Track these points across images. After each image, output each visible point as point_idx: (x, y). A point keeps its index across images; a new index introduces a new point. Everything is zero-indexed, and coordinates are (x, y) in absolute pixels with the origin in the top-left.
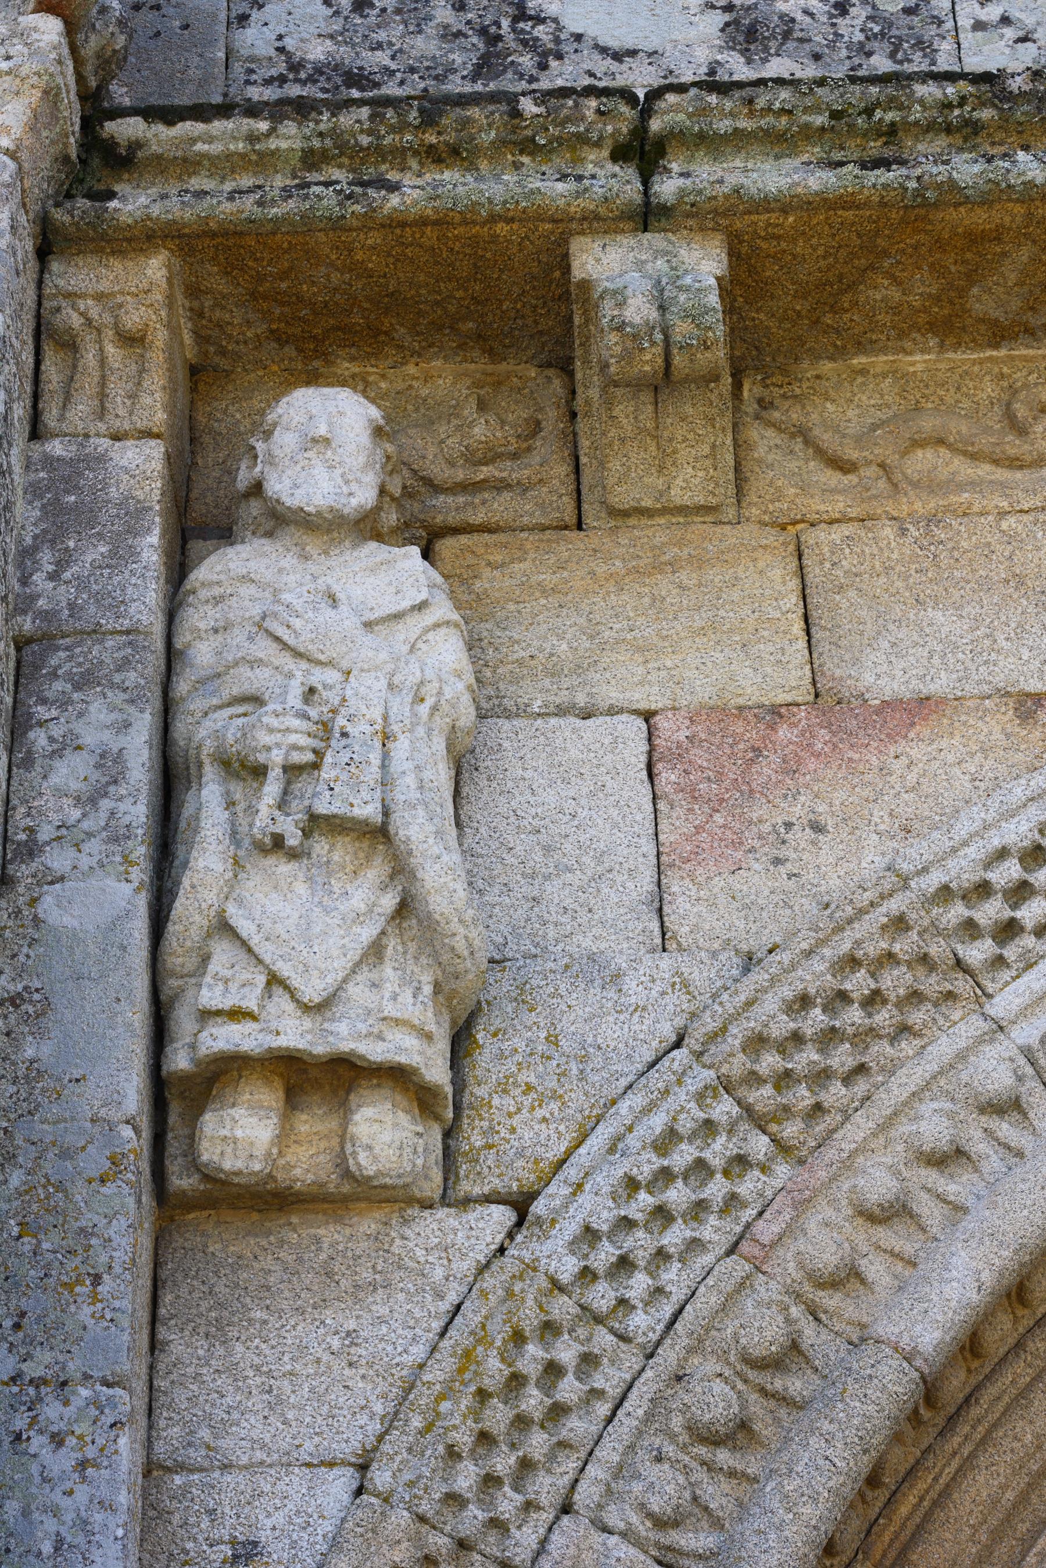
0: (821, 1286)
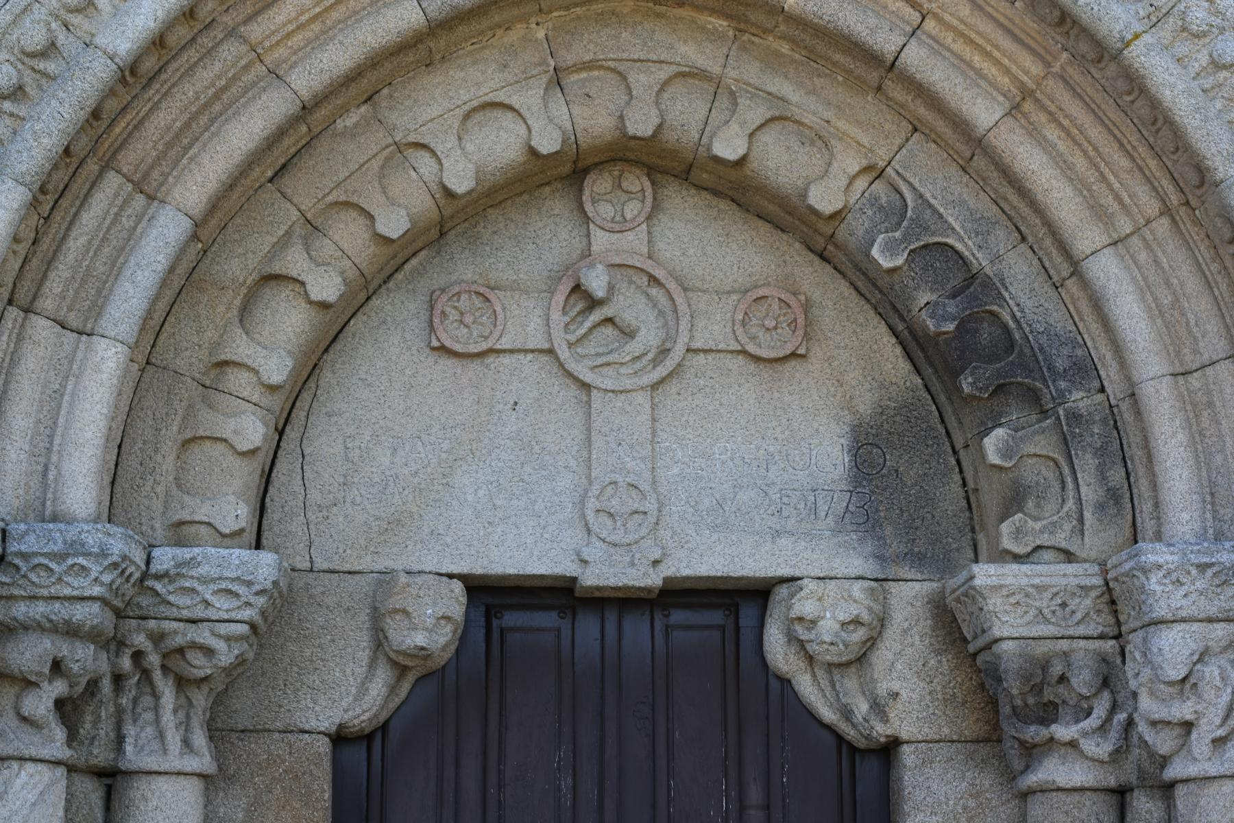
0: (71, 12)
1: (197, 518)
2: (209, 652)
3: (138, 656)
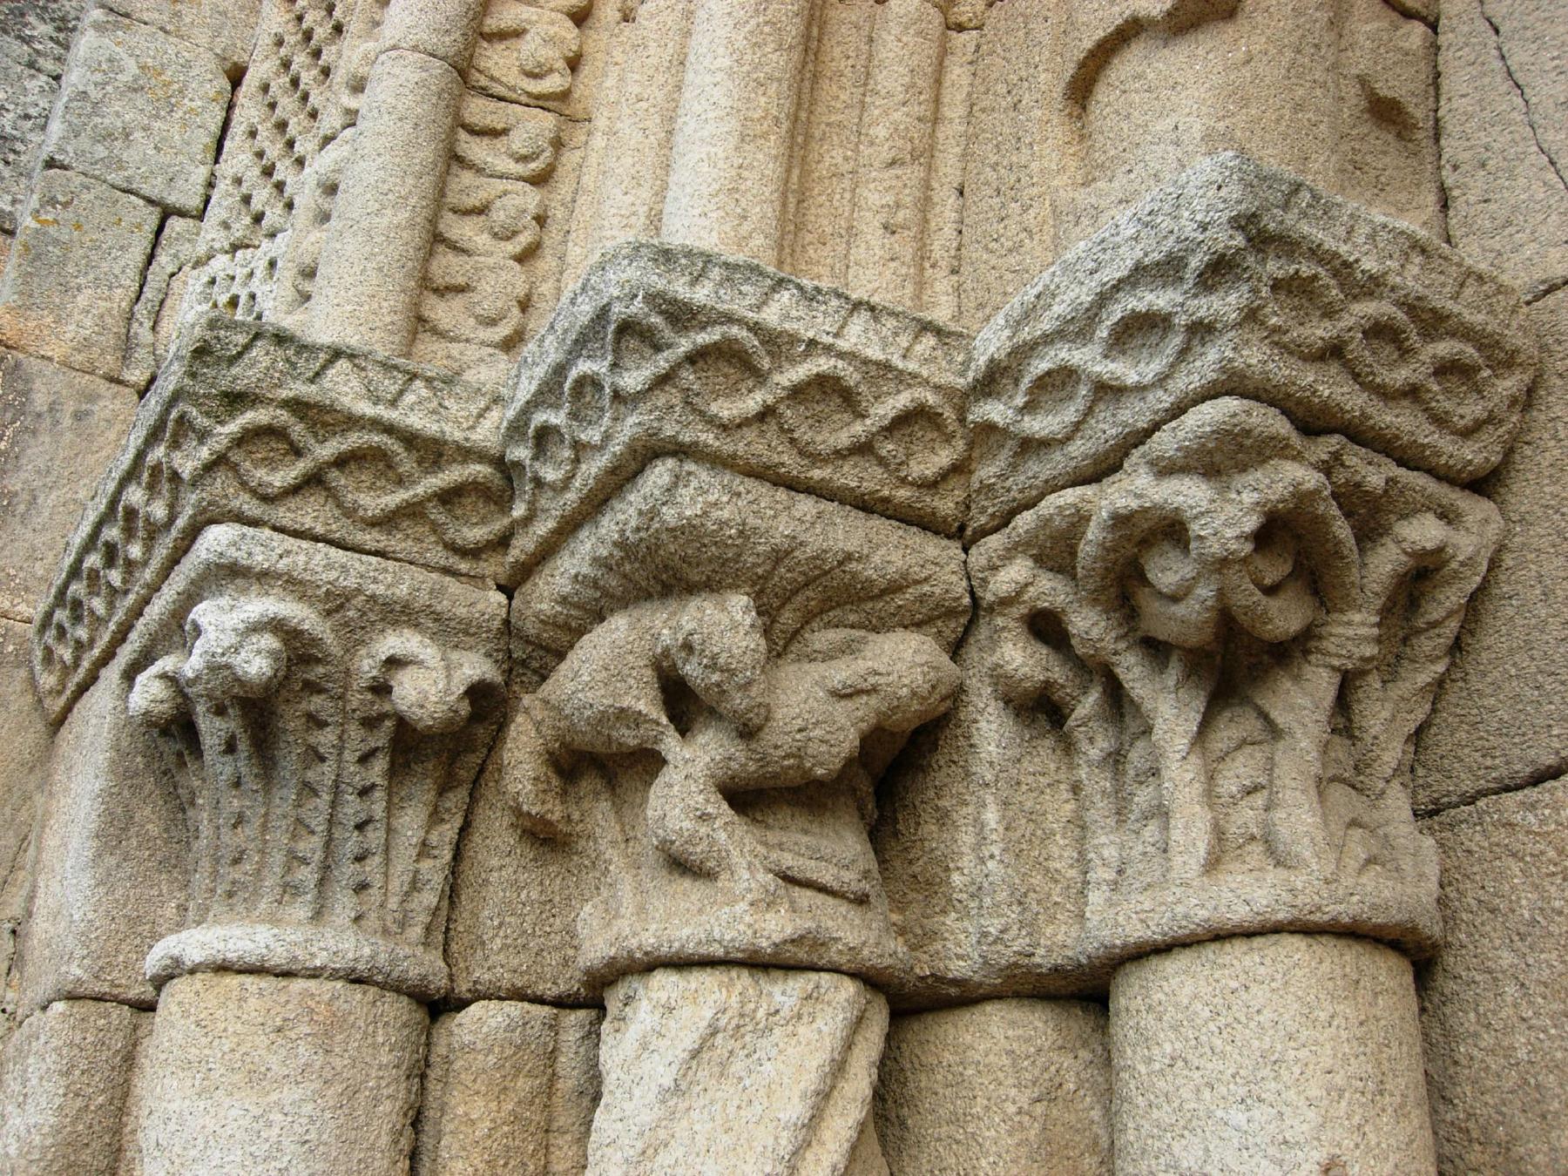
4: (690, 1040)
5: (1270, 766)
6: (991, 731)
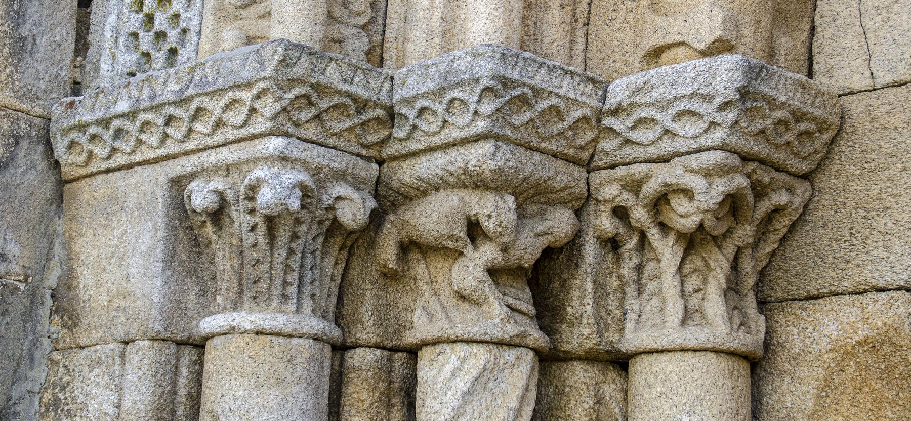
1: (670, 39)
2: (688, 193)
3: (621, 213)
4: (475, 373)
5: (705, 282)
6: (590, 251)
